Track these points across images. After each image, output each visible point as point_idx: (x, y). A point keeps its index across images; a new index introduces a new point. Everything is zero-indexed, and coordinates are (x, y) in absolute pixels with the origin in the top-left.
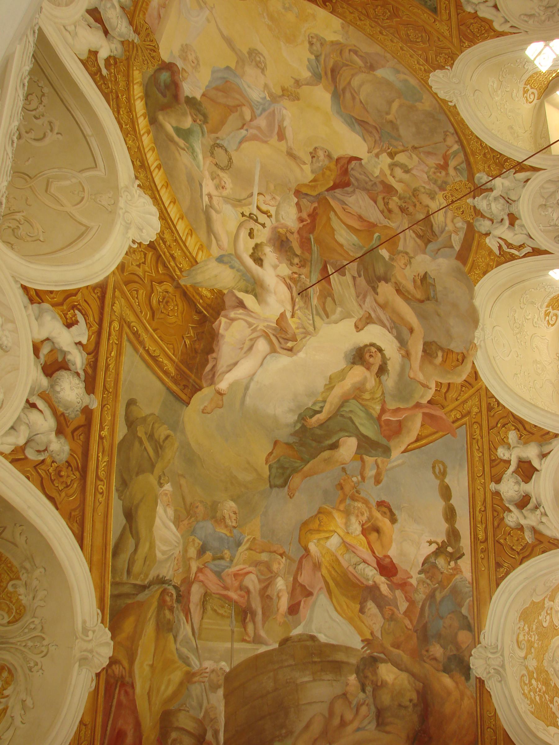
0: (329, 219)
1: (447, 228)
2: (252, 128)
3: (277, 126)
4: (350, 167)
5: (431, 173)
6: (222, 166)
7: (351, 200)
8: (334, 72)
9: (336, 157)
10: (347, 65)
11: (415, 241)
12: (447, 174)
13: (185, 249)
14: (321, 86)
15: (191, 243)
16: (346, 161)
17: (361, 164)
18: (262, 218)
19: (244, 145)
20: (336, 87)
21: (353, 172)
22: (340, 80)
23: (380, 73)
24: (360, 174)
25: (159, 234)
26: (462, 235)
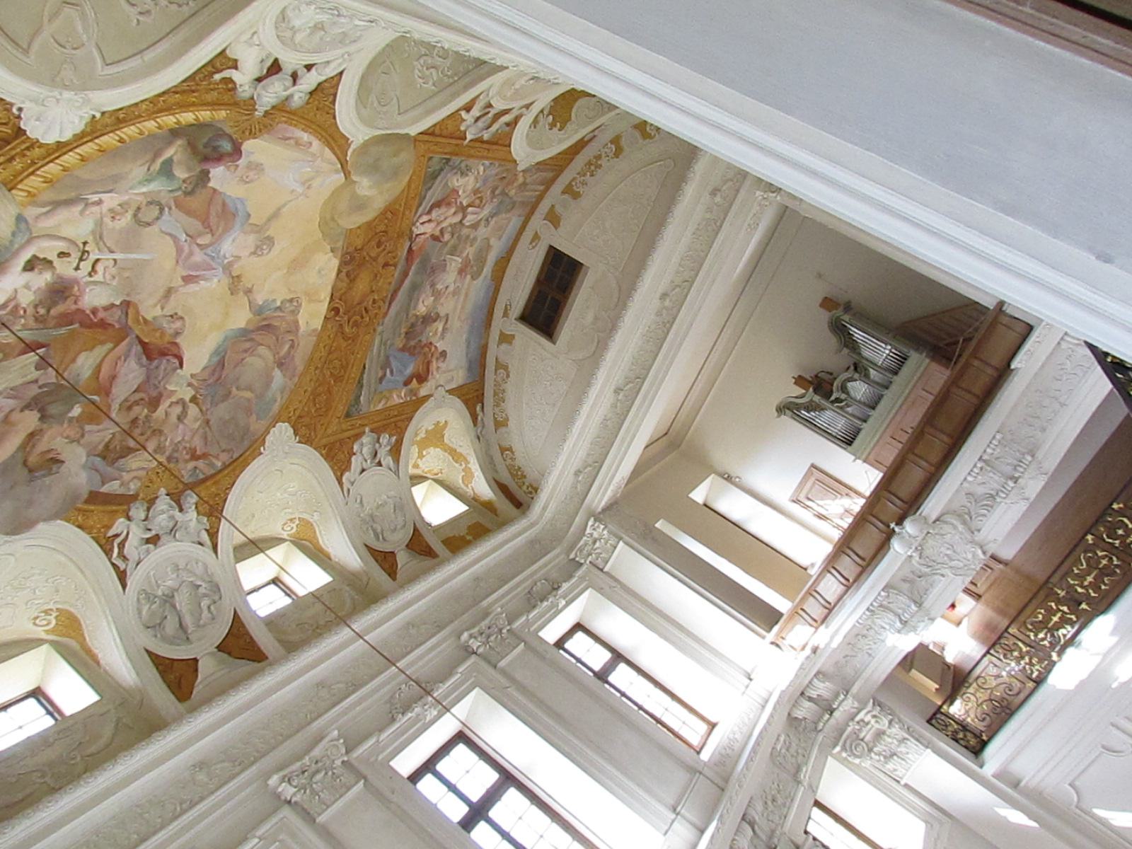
0: (102, 343)
1: (124, 474)
2: (190, 246)
3: (198, 273)
4: (169, 357)
5: (184, 444)
6: (140, 215)
7: (132, 363)
8: (268, 328)
9: (178, 341)
10: (277, 339)
11: (99, 443)
12: (187, 461)
13: (26, 173)
14: (251, 315)
15: (34, 182)
16: (176, 352)
17: (176, 369)
18: (86, 266)
19: (168, 238)
20: (253, 331)
21: (165, 361)
23: (277, 374)
24: (165, 369)
25: (38, 141)
26: (121, 491)
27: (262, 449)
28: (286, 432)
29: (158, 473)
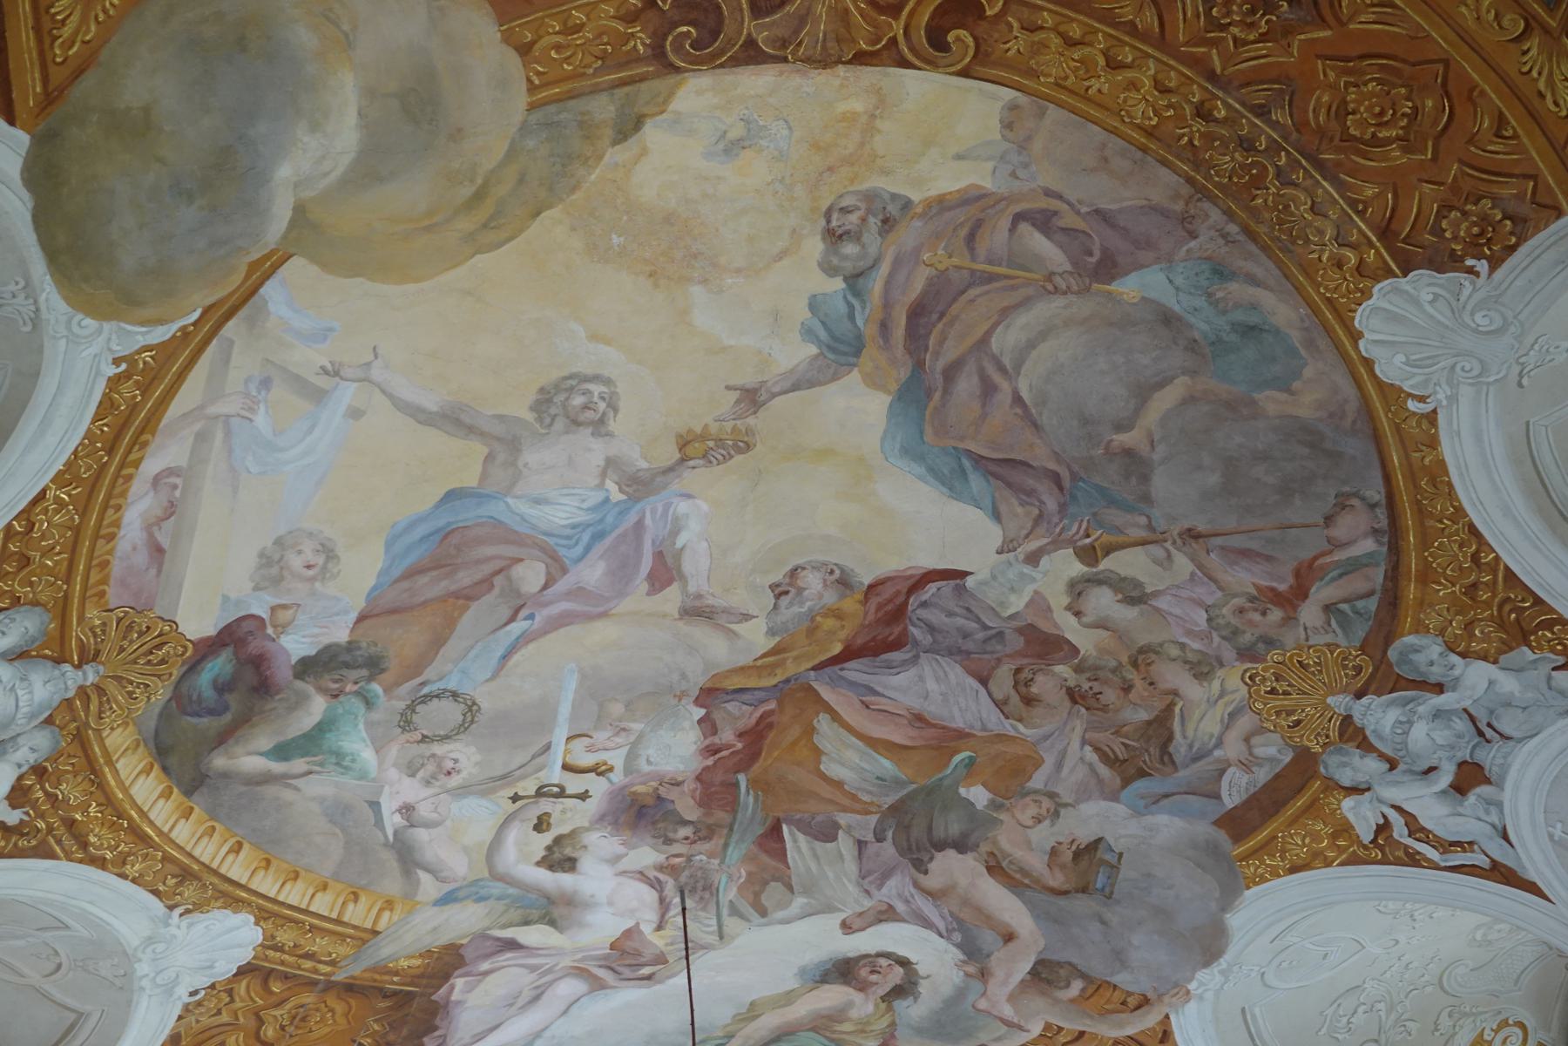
10: (992, 278)
20: (919, 365)
22: (943, 340)
27: (1412, 405)
28: (1416, 302)
29: (1273, 691)
